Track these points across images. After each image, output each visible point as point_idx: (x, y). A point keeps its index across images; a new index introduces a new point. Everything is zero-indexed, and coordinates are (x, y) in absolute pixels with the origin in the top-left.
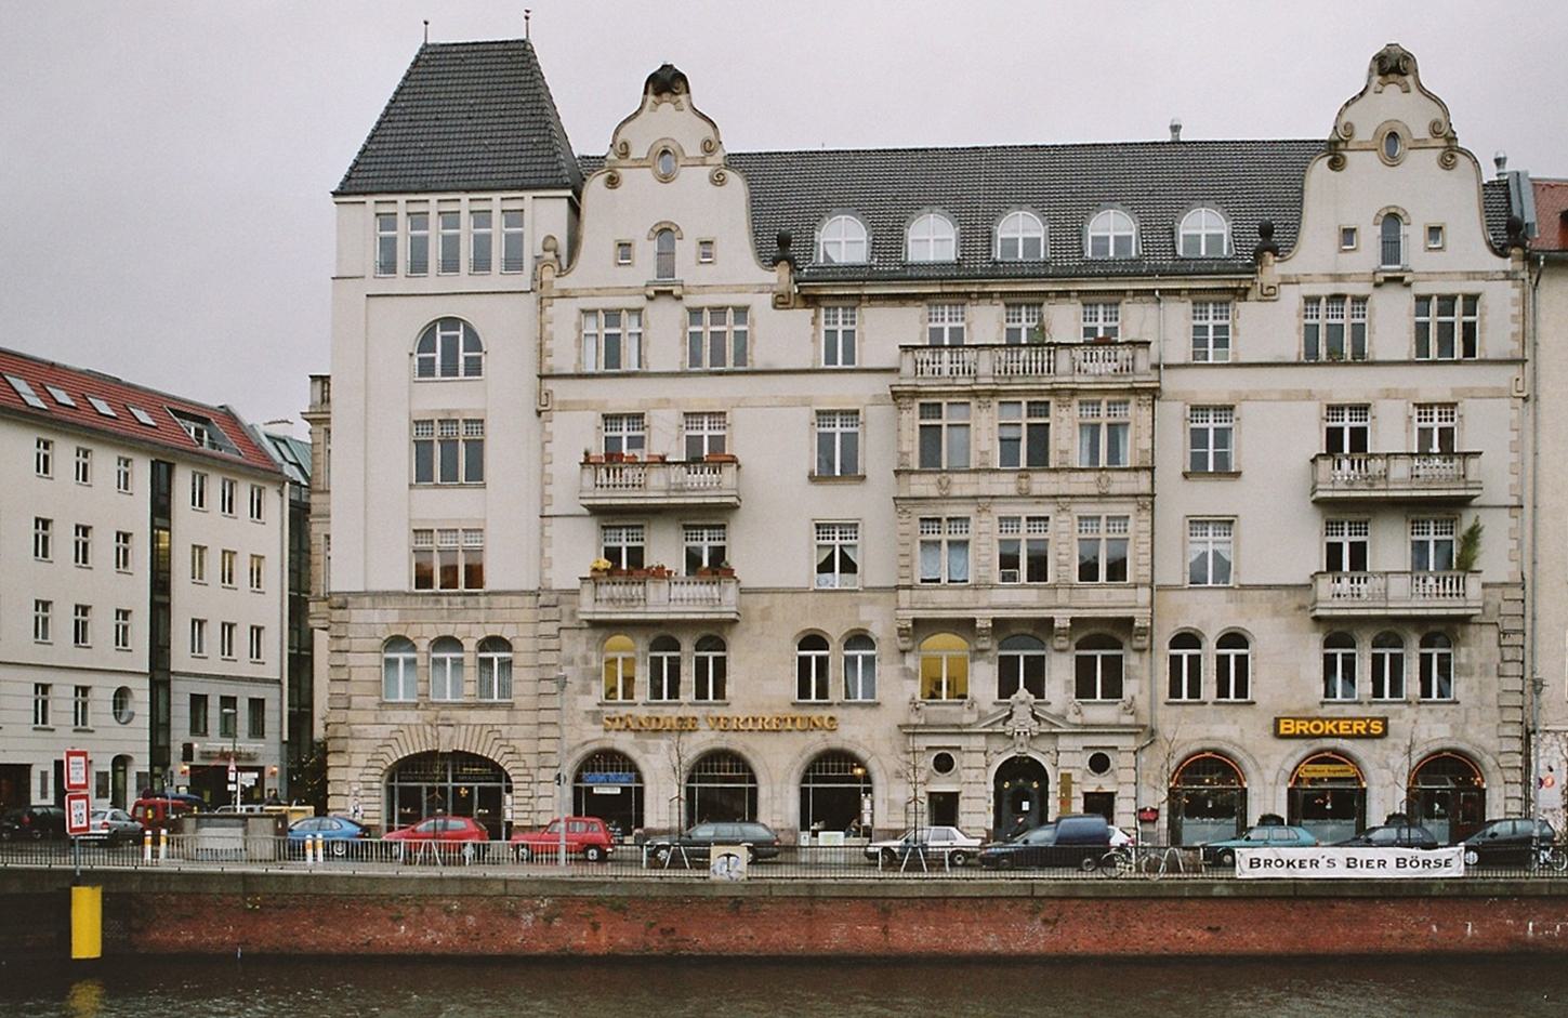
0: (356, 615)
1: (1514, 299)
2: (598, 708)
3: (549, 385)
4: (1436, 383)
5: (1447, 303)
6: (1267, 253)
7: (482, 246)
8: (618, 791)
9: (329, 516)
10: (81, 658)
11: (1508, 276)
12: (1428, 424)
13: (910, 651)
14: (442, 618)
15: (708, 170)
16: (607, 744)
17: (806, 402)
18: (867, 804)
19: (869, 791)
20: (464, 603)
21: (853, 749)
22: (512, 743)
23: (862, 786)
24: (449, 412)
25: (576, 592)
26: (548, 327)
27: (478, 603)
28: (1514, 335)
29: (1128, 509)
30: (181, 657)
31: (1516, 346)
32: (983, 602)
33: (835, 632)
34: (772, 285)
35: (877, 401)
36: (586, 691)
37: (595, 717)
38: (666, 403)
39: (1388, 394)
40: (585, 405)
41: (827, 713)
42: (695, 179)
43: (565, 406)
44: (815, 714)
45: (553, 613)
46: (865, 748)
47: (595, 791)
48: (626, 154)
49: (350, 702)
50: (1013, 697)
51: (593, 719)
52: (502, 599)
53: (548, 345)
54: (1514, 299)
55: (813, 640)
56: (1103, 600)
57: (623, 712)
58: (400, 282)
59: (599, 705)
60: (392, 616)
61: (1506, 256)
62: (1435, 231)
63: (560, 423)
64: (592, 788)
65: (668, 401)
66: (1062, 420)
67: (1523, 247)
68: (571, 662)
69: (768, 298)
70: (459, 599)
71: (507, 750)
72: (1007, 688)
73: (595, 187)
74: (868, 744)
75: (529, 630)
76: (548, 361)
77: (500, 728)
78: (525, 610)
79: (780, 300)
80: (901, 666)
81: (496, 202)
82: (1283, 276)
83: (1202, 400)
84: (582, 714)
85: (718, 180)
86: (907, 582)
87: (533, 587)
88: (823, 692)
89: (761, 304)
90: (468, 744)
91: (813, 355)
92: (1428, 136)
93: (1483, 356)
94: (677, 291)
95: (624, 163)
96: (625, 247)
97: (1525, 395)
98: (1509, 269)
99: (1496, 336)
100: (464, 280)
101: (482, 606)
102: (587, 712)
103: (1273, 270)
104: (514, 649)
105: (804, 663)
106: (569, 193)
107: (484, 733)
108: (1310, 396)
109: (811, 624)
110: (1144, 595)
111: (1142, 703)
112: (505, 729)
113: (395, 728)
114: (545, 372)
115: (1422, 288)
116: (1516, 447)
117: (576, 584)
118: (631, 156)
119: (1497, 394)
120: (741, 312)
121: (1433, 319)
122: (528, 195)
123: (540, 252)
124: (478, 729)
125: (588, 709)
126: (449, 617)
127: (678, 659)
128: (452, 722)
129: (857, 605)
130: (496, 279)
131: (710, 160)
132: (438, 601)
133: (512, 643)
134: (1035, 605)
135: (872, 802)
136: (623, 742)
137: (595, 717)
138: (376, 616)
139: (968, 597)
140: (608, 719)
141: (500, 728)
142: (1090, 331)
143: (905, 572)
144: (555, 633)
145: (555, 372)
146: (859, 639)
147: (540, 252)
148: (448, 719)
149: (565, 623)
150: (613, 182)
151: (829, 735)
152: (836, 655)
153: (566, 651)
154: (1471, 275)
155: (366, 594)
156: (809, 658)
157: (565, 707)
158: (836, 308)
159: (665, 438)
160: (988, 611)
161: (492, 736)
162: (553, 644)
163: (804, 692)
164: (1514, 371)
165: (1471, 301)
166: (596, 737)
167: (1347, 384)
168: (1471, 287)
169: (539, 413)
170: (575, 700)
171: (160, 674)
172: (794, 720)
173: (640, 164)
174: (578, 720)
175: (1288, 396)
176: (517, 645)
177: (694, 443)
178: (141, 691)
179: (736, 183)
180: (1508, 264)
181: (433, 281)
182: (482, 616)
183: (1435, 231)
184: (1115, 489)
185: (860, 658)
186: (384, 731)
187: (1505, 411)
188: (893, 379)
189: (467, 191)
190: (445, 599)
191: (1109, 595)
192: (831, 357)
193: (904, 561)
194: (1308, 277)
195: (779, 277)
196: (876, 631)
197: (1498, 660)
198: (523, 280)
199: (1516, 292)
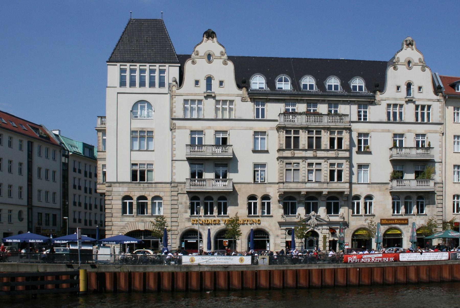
0: (115, 189)
1: (440, 107)
3: (174, 122)
4: (421, 129)
5: (423, 107)
6: (377, 92)
7: (152, 80)
8: (195, 241)
9: (105, 159)
10: (10, 201)
11: (438, 101)
12: (418, 140)
13: (281, 201)
14: (141, 190)
15: (222, 60)
17: (250, 129)
18: (268, 245)
19: (268, 241)
20: (148, 186)
21: (265, 229)
23: (266, 239)
24: (143, 128)
25: (185, 183)
26: (174, 104)
27: (152, 186)
28: (440, 116)
29: (343, 161)
30: (35, 202)
31: (440, 119)
32: (304, 187)
33: (259, 195)
34: (241, 94)
35: (271, 129)
36: (186, 212)
38: (209, 128)
39: (409, 131)
40: (185, 128)
41: (257, 219)
42: (217, 63)
43: (180, 128)
44: (254, 219)
45: (176, 189)
46: (268, 228)
47: (188, 241)
48: (198, 54)
49: (112, 215)
50: (310, 214)
51: (188, 220)
52: (160, 184)
53: (174, 109)
54: (440, 107)
55: (252, 197)
56: (336, 187)
57: (197, 218)
58: (127, 89)
60: (126, 189)
61: (438, 95)
62: (420, 88)
63: (177, 133)
64: (187, 241)
65: (210, 127)
66: (325, 136)
67: (442, 93)
68: (181, 204)
69: (240, 98)
70: (146, 185)
72: (308, 212)
73: (188, 65)
74: (269, 227)
75: (169, 194)
76: (174, 114)
78: (168, 188)
79: (243, 99)
80: (278, 205)
81: (157, 67)
82: (382, 98)
83: (418, 132)
85: (225, 63)
86: (282, 181)
87: (170, 181)
88: (255, 213)
89: (238, 100)
91: (252, 115)
92: (418, 62)
93: (432, 122)
94: (213, 95)
95: (197, 57)
96: (197, 82)
97: (443, 132)
98: (439, 99)
99: (435, 115)
100: (147, 89)
102: (186, 218)
103: (379, 96)
104: (148, 199)
105: (250, 204)
106: (180, 65)
108: (389, 131)
109: (252, 193)
110: (347, 185)
111: (345, 216)
113: (127, 223)
114: (173, 117)
115: (417, 103)
116: (441, 146)
117: (185, 181)
118: (199, 55)
119: (435, 132)
120: (231, 102)
121: (419, 111)
122: (167, 65)
123: (171, 82)
125: (187, 217)
126: (143, 189)
127: (226, 203)
128: (144, 221)
129: (266, 187)
130: (157, 89)
131: (222, 57)
132: (140, 185)
133: (163, 197)
134: (318, 188)
135: (269, 244)
137: (189, 220)
138: (120, 189)
139: (299, 185)
140: (193, 220)
142: (330, 111)
143: (282, 178)
144: (179, 195)
145: (176, 118)
146: (266, 197)
147: (171, 82)
148: (143, 220)
149: (180, 192)
150: (194, 63)
152: (259, 201)
153: (180, 201)
154: (430, 100)
155: (117, 182)
156: (251, 203)
157: (179, 217)
158: (259, 102)
159: (209, 139)
160: (305, 190)
162: (176, 198)
163: (250, 212)
164: (440, 126)
165: (429, 107)
166: (188, 225)
167: (398, 128)
168: (429, 103)
169: (171, 130)
170: (182, 214)
171: (30, 206)
172: (248, 221)
173: (202, 58)
174: (184, 221)
175: (383, 131)
176: (164, 198)
177: (217, 139)
178: (25, 211)
179: (231, 65)
180: (438, 97)
181: (137, 89)
182: (153, 189)
183: (420, 88)
184: (340, 156)
185: (266, 203)
186: (123, 224)
187: (438, 136)
188: (276, 123)
189: (149, 63)
190: (142, 185)
191: (338, 185)
192: (258, 116)
193: (281, 175)
194: (388, 99)
195: (243, 92)
196: (271, 194)
198: (165, 90)
199: (440, 105)
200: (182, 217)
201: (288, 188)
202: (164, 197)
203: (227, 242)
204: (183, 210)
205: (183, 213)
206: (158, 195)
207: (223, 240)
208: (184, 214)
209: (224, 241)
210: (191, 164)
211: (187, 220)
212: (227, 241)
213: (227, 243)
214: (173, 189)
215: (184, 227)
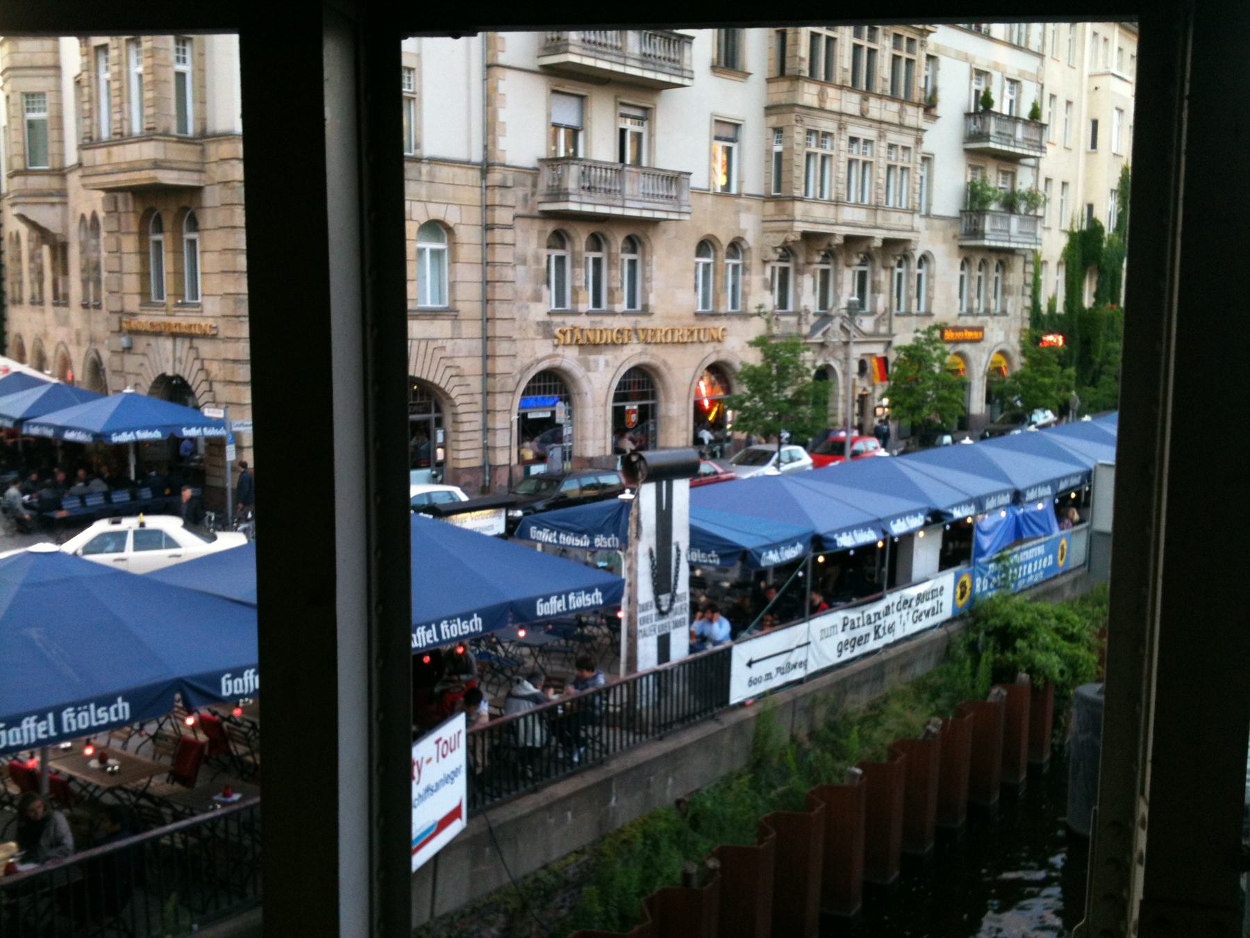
2: (547, 318)
16: (557, 362)
22: (458, 362)
36: (537, 298)
37: (546, 329)
59: (549, 314)
68: (524, 262)
71: (454, 372)
77: (444, 343)
84: (535, 327)
90: (426, 370)
101: (424, 178)
107: (430, 351)
112: (449, 344)
124: (423, 344)
136: (569, 359)
137: (546, 329)
141: (444, 343)
149: (520, 210)
151: (718, 346)
161: (439, 354)
170: (527, 307)
174: (531, 333)
196: (750, 239)
197: (1022, 283)
200: (525, 320)
201: (810, 219)
202: (462, 227)
203: (634, 411)
204: (528, 289)
205: (528, 300)
206: (440, 216)
207: (624, 407)
208: (532, 306)
209: (627, 408)
210: (554, 92)
211: (541, 330)
212: (635, 407)
213: (634, 418)
214: (502, 195)
215: (532, 359)
